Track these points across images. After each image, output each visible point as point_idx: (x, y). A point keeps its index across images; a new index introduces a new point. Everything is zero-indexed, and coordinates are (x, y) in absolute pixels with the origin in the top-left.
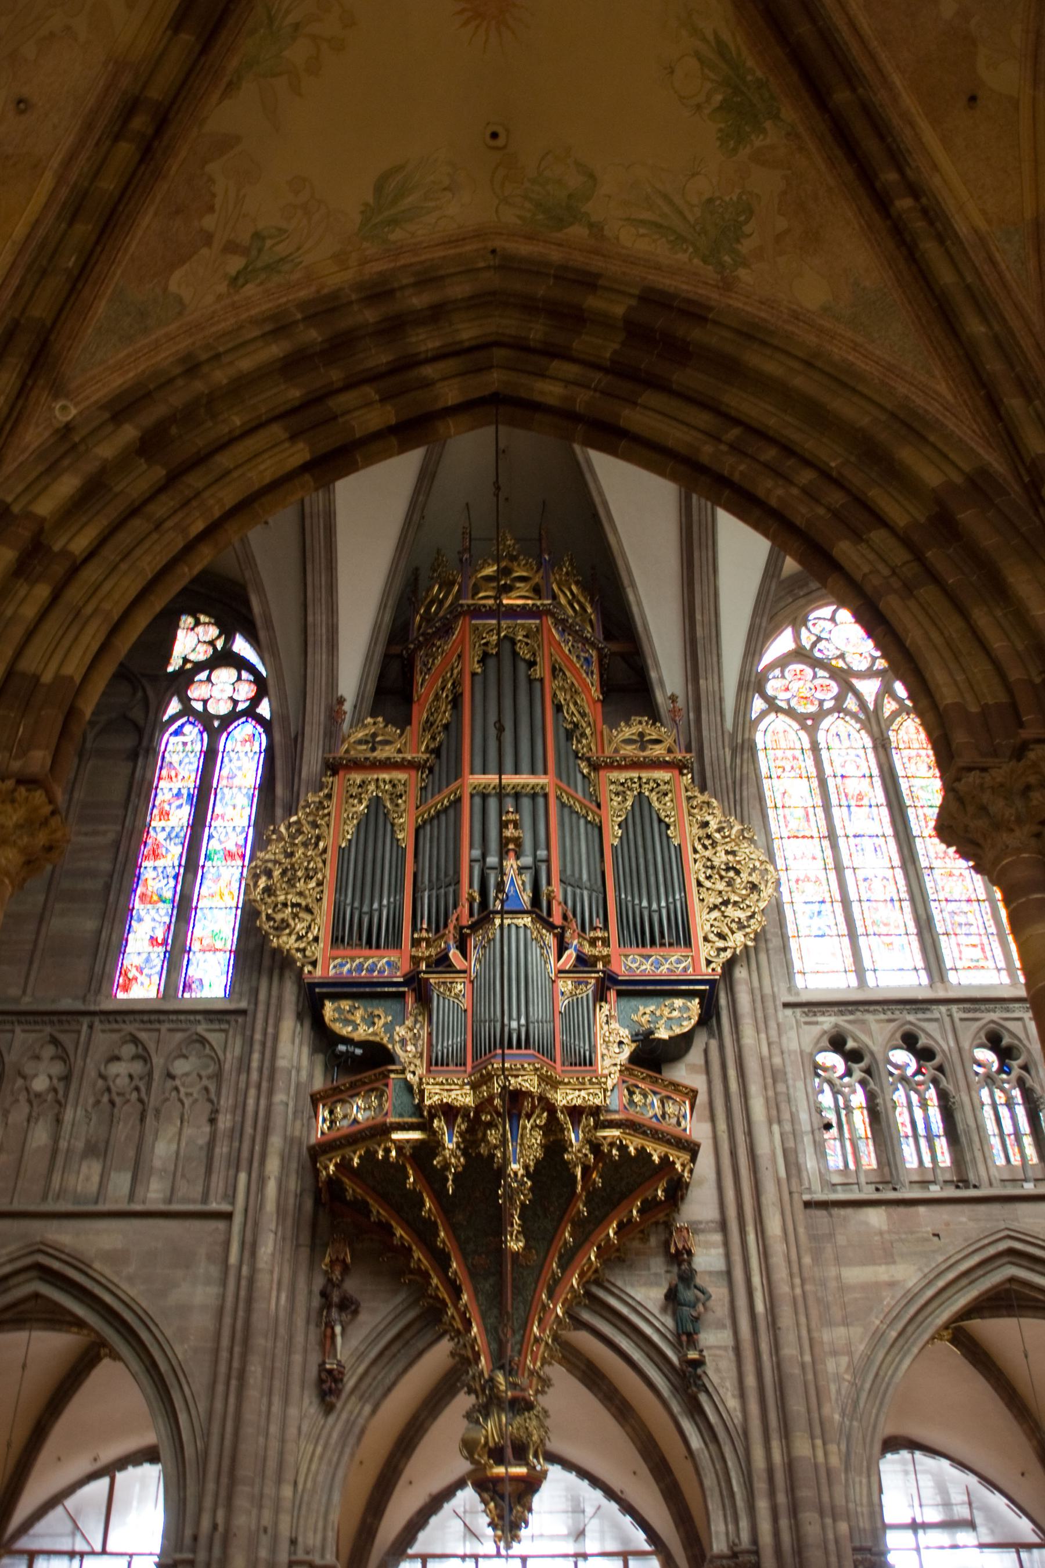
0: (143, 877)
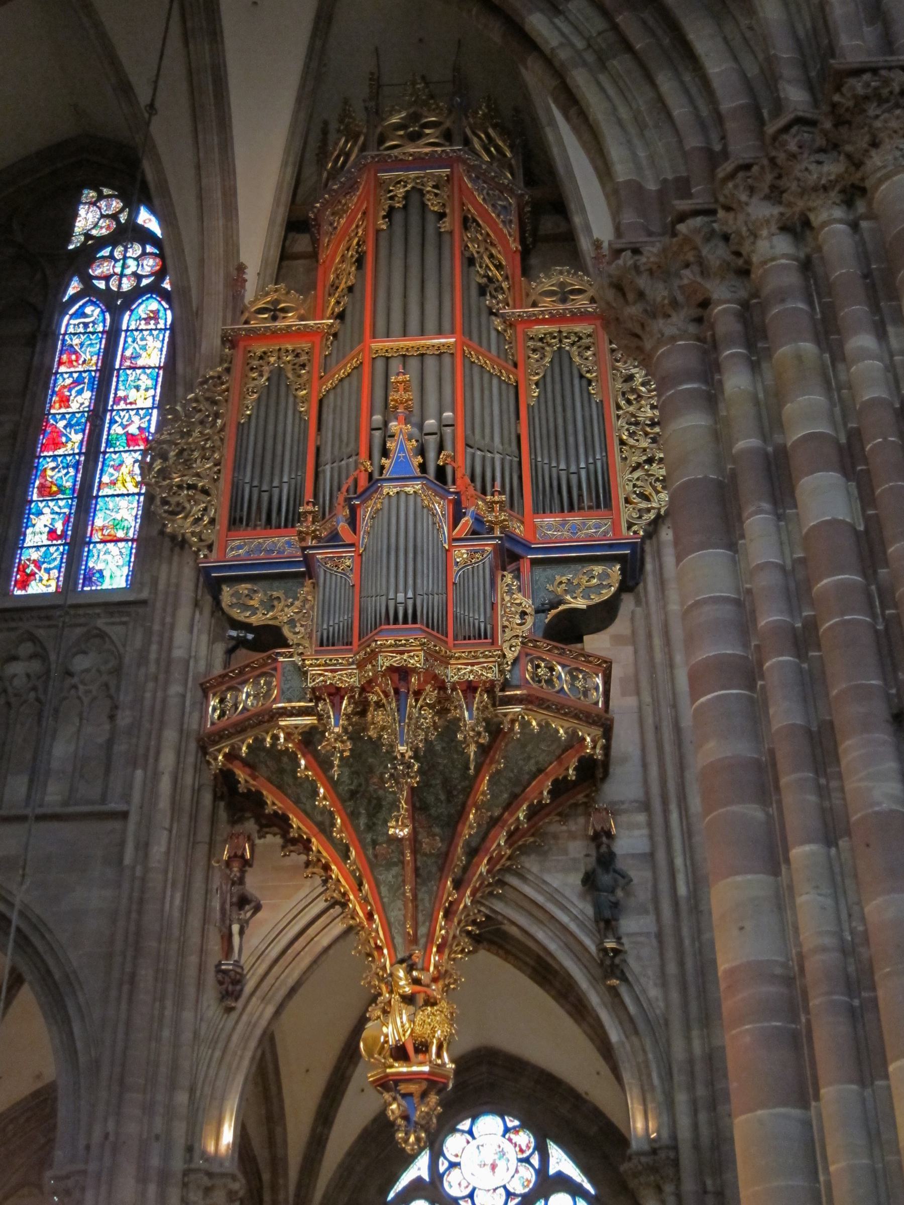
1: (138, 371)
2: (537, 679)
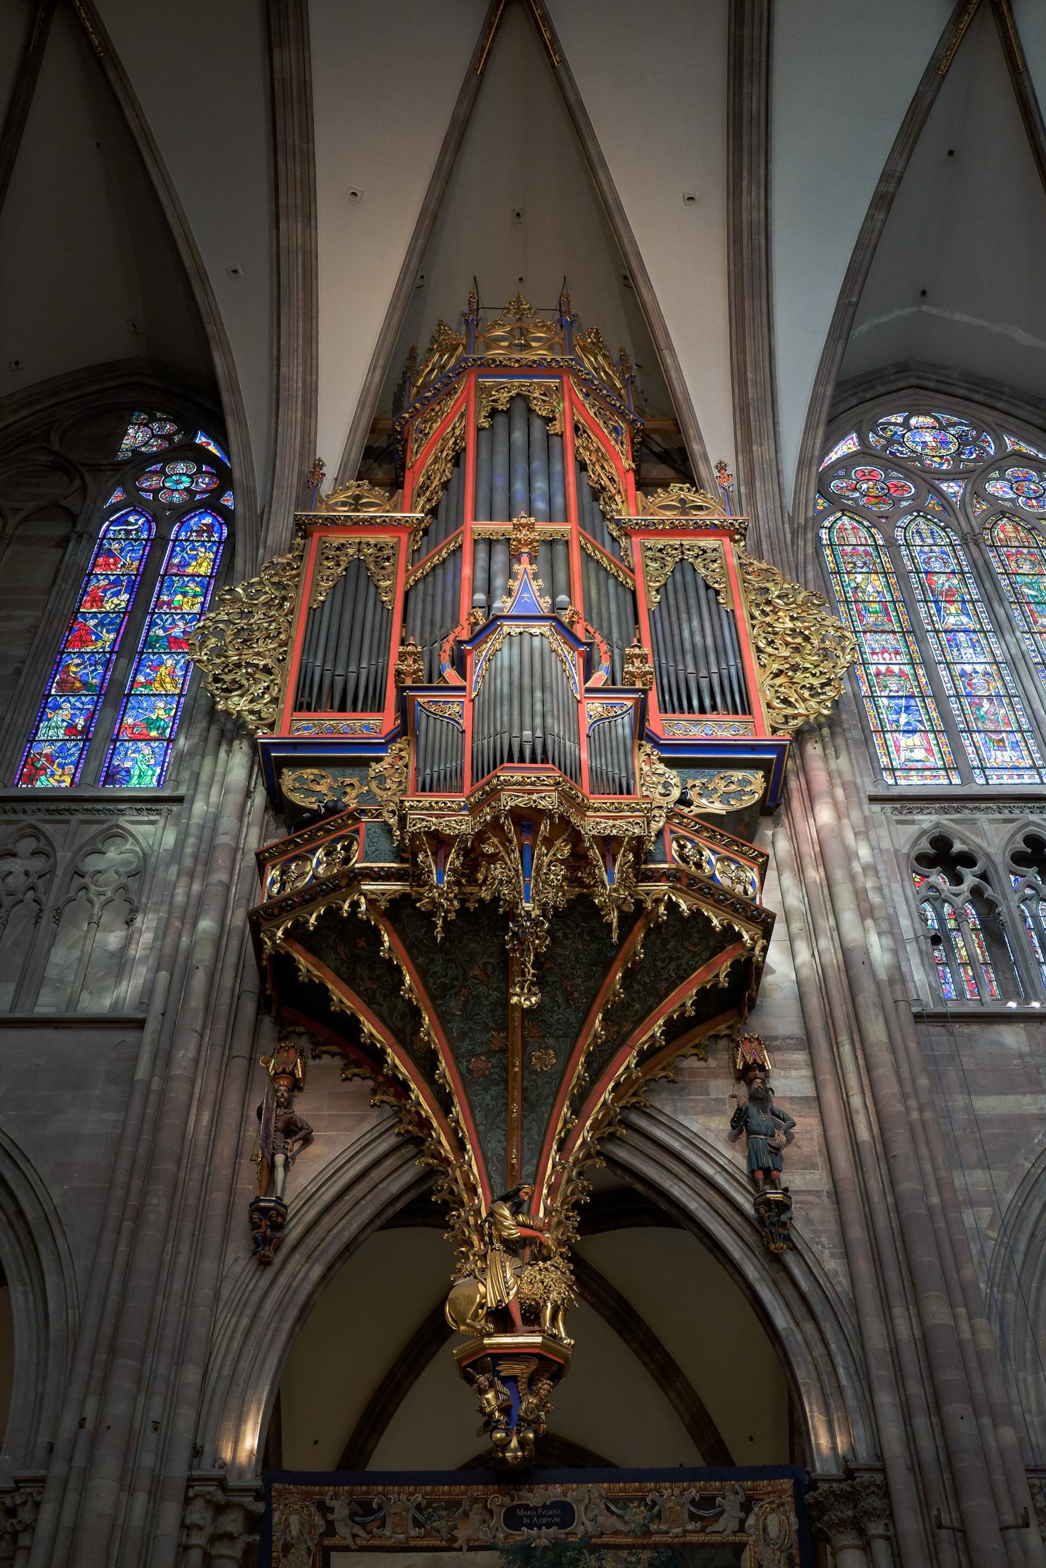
1: (186, 579)
2: (684, 859)
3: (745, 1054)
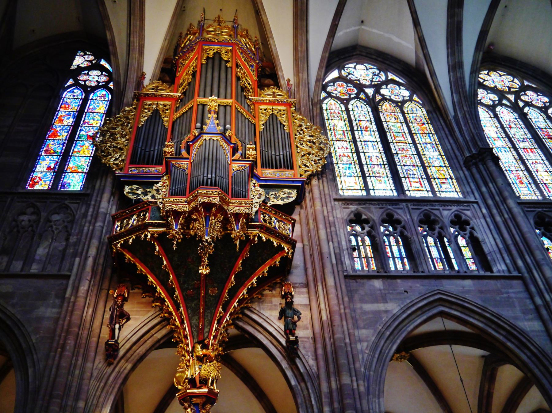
0: (47, 143)
1: (95, 114)
3: (285, 290)
